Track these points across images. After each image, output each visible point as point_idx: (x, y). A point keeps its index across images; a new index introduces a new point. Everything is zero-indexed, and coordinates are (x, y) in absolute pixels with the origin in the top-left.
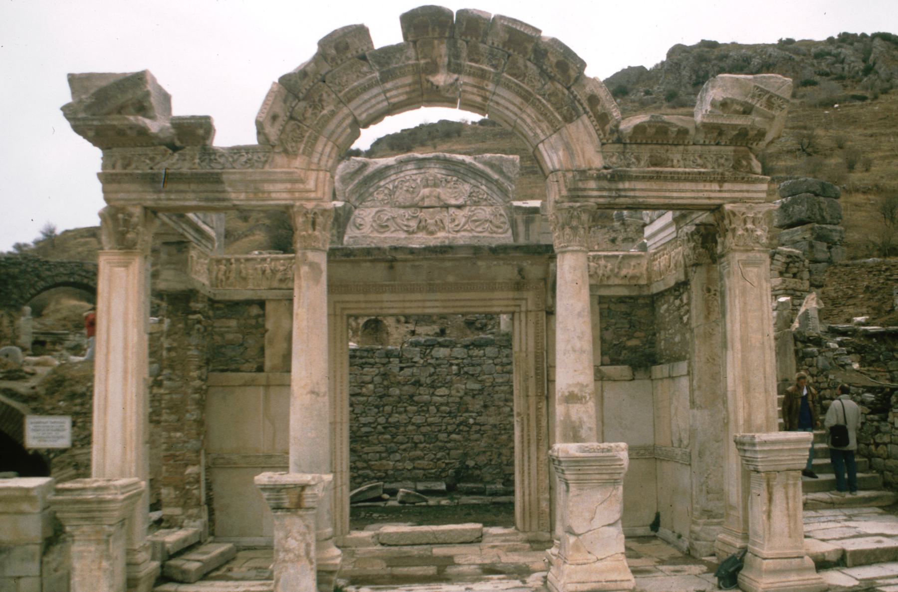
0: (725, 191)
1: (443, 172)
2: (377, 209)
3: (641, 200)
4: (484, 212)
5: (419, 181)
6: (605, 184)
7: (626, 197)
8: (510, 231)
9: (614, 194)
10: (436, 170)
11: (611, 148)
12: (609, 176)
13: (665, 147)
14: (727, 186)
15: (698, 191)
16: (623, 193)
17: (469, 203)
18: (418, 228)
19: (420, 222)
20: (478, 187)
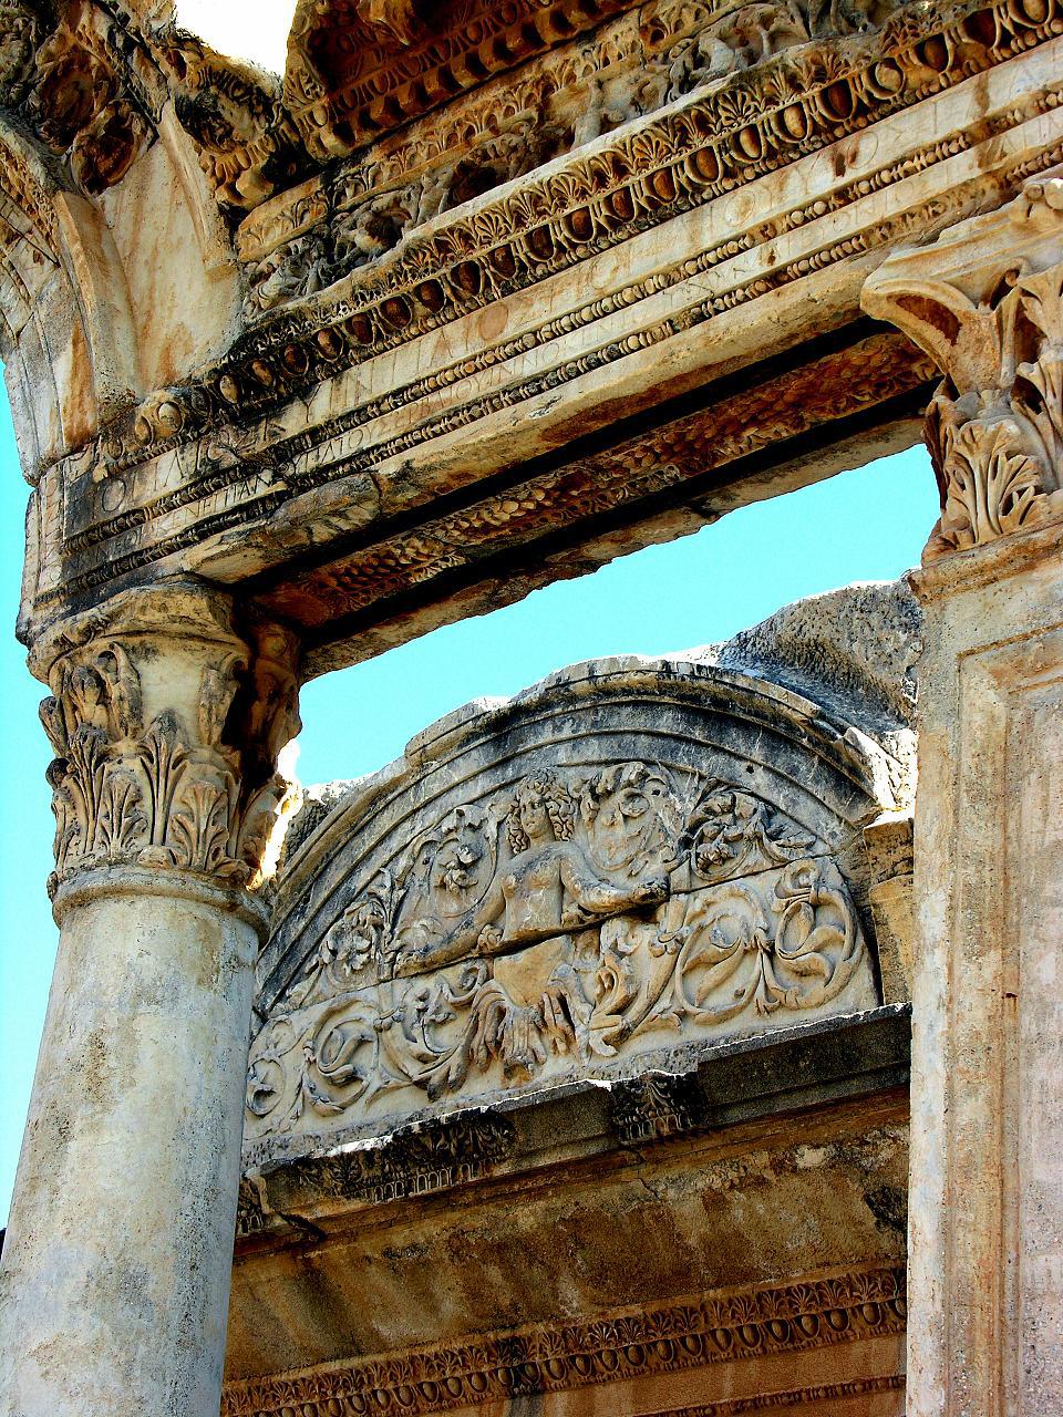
0: (876, 184)
1: (593, 750)
2: (322, 1008)
3: (389, 467)
4: (742, 905)
5: (491, 829)
6: (226, 446)
7: (321, 475)
8: (864, 977)
9: (262, 486)
10: (563, 755)
11: (274, 224)
12: (227, 389)
13: (530, 75)
14: (876, 145)
15: (701, 264)
16: (305, 464)
17: (680, 877)
18: (469, 1056)
19: (475, 1029)
20: (732, 786)
